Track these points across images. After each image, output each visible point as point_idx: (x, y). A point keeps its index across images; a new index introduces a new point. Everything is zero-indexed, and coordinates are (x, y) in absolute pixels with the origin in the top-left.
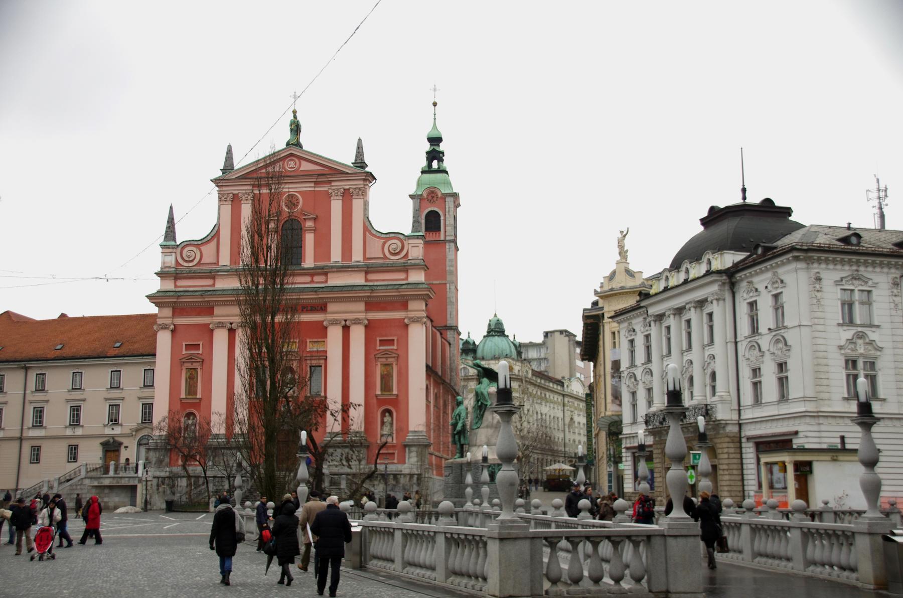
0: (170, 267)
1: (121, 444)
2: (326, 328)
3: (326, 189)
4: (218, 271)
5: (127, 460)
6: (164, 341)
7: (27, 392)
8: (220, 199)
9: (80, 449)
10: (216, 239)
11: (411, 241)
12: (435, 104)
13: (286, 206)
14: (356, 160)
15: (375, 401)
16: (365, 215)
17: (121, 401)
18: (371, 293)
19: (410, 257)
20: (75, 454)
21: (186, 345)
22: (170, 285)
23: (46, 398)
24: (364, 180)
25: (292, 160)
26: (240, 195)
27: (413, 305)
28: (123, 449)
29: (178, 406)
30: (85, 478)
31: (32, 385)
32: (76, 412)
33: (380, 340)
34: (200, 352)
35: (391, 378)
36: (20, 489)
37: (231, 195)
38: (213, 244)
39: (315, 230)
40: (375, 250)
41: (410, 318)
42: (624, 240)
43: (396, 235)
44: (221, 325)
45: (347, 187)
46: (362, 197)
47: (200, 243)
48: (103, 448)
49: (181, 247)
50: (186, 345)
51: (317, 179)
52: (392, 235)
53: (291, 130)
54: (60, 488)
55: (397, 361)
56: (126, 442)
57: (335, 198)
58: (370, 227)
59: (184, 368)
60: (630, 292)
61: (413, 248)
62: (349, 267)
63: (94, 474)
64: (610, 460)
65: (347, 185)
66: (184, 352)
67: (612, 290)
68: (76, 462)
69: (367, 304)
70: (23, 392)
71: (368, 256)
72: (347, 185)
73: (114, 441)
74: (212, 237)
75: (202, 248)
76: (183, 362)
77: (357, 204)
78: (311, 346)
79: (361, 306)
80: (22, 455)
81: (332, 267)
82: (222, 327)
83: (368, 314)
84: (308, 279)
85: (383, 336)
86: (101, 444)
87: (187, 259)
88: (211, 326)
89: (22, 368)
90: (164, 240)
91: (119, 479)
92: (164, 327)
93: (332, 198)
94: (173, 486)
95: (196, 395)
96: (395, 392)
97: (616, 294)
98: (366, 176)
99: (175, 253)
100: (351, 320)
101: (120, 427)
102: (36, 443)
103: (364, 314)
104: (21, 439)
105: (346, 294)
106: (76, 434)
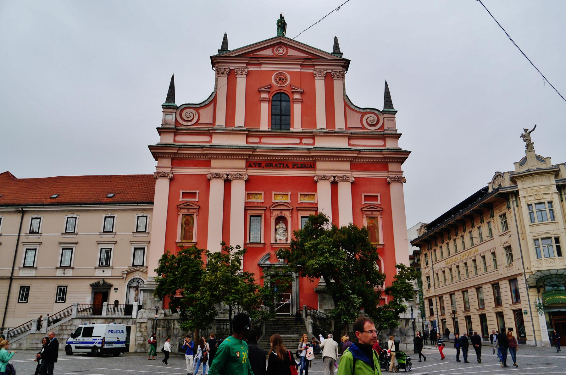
0: (170, 124)
1: (111, 286)
2: (316, 182)
3: (312, 71)
5: (117, 302)
7: (21, 234)
8: (218, 73)
10: (212, 105)
11: (385, 115)
13: (276, 81)
14: (334, 51)
17: (113, 245)
18: (358, 154)
19: (386, 128)
20: (63, 295)
21: (183, 193)
22: (169, 139)
23: (39, 241)
24: (343, 66)
25: (280, 47)
26: (236, 70)
28: (112, 289)
30: (76, 318)
31: (26, 229)
33: (365, 196)
34: (197, 200)
35: (376, 230)
36: (6, 328)
37: (228, 70)
38: (211, 108)
40: (354, 121)
41: (391, 178)
42: (530, 135)
43: (372, 111)
44: (218, 176)
45: (330, 71)
46: (341, 79)
47: (198, 106)
48: (92, 290)
49: (180, 109)
50: (183, 193)
51: (303, 62)
52: (368, 110)
53: (279, 27)
54: (49, 328)
55: (382, 214)
56: (115, 284)
57: (319, 78)
58: (349, 103)
59: (181, 214)
60: (544, 173)
61: (388, 121)
62: (335, 133)
63: (86, 314)
64: (540, 308)
65: (329, 69)
66: (181, 199)
67: (529, 170)
68: (64, 302)
69: (352, 164)
70: (18, 234)
71: (349, 125)
72: (329, 69)
73: (104, 283)
74: (210, 103)
75: (201, 111)
76: (181, 208)
77: (337, 84)
78: (302, 199)
79: (347, 166)
80: (11, 295)
81: (320, 132)
82: (219, 177)
83: (353, 173)
84: (297, 141)
85: (368, 192)
86: (90, 285)
87: (186, 119)
88: (208, 176)
89: (19, 212)
90: (166, 102)
91: (112, 320)
93: (316, 78)
94: (169, 329)
95: (192, 240)
96: (381, 242)
97: (531, 175)
98: (345, 63)
99: (175, 112)
100: (339, 177)
101: (111, 270)
102: (25, 283)
103: (351, 172)
104: (11, 279)
106: (66, 275)
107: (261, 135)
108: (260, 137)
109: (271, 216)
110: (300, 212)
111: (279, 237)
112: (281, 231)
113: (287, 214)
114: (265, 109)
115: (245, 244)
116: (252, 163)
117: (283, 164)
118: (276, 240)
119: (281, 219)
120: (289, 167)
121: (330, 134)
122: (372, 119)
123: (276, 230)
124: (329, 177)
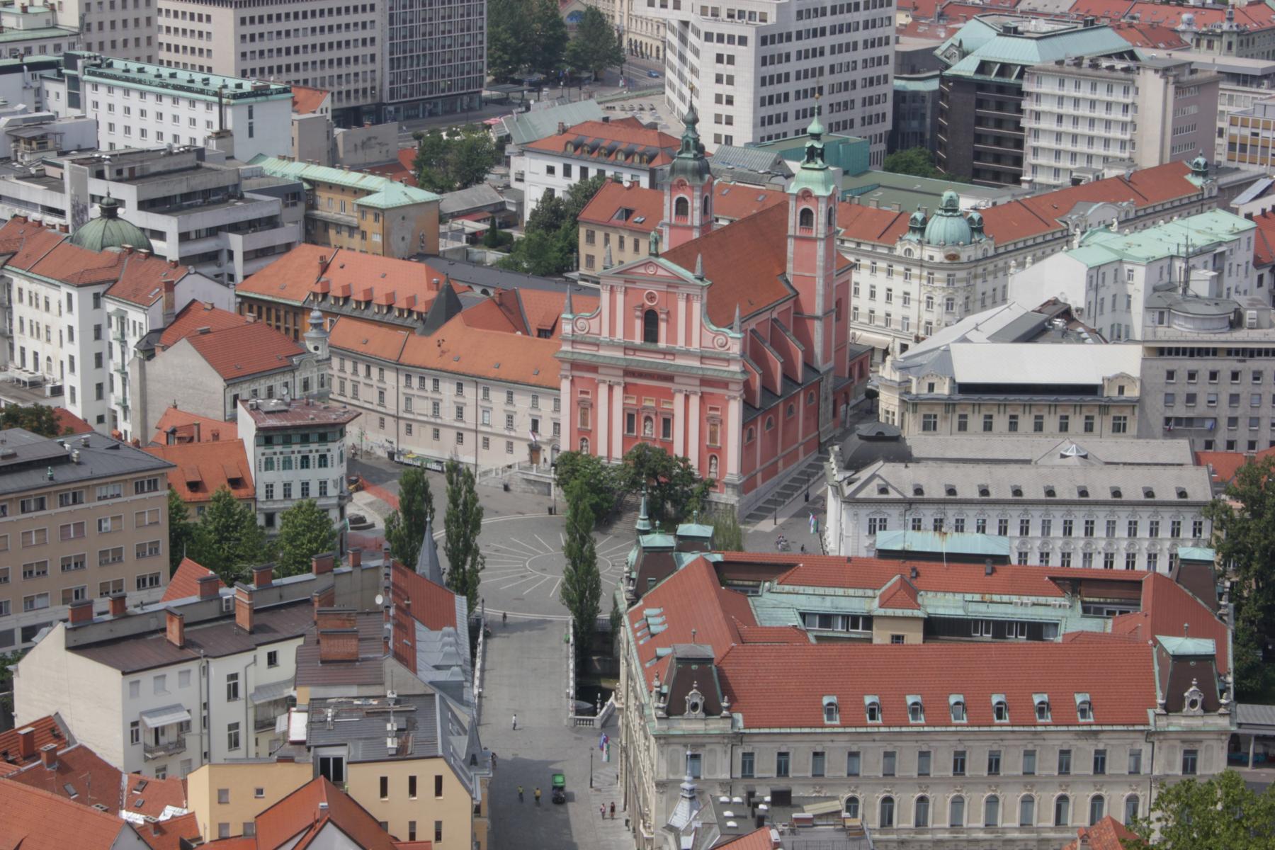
5: (545, 460)
6: (565, 385)
9: (514, 445)
15: (705, 449)
27: (732, 386)
29: (576, 432)
32: (510, 418)
34: (589, 397)
39: (667, 321)
40: (707, 342)
56: (544, 447)
65: (691, 291)
72: (691, 291)
79: (697, 382)
84: (662, 356)
92: (566, 377)
104: (476, 431)
105: (687, 373)
107: (635, 349)
111: (647, 432)
112: (648, 428)
113: (653, 417)
115: (623, 435)
119: (648, 418)
121: (687, 354)
122: (720, 341)
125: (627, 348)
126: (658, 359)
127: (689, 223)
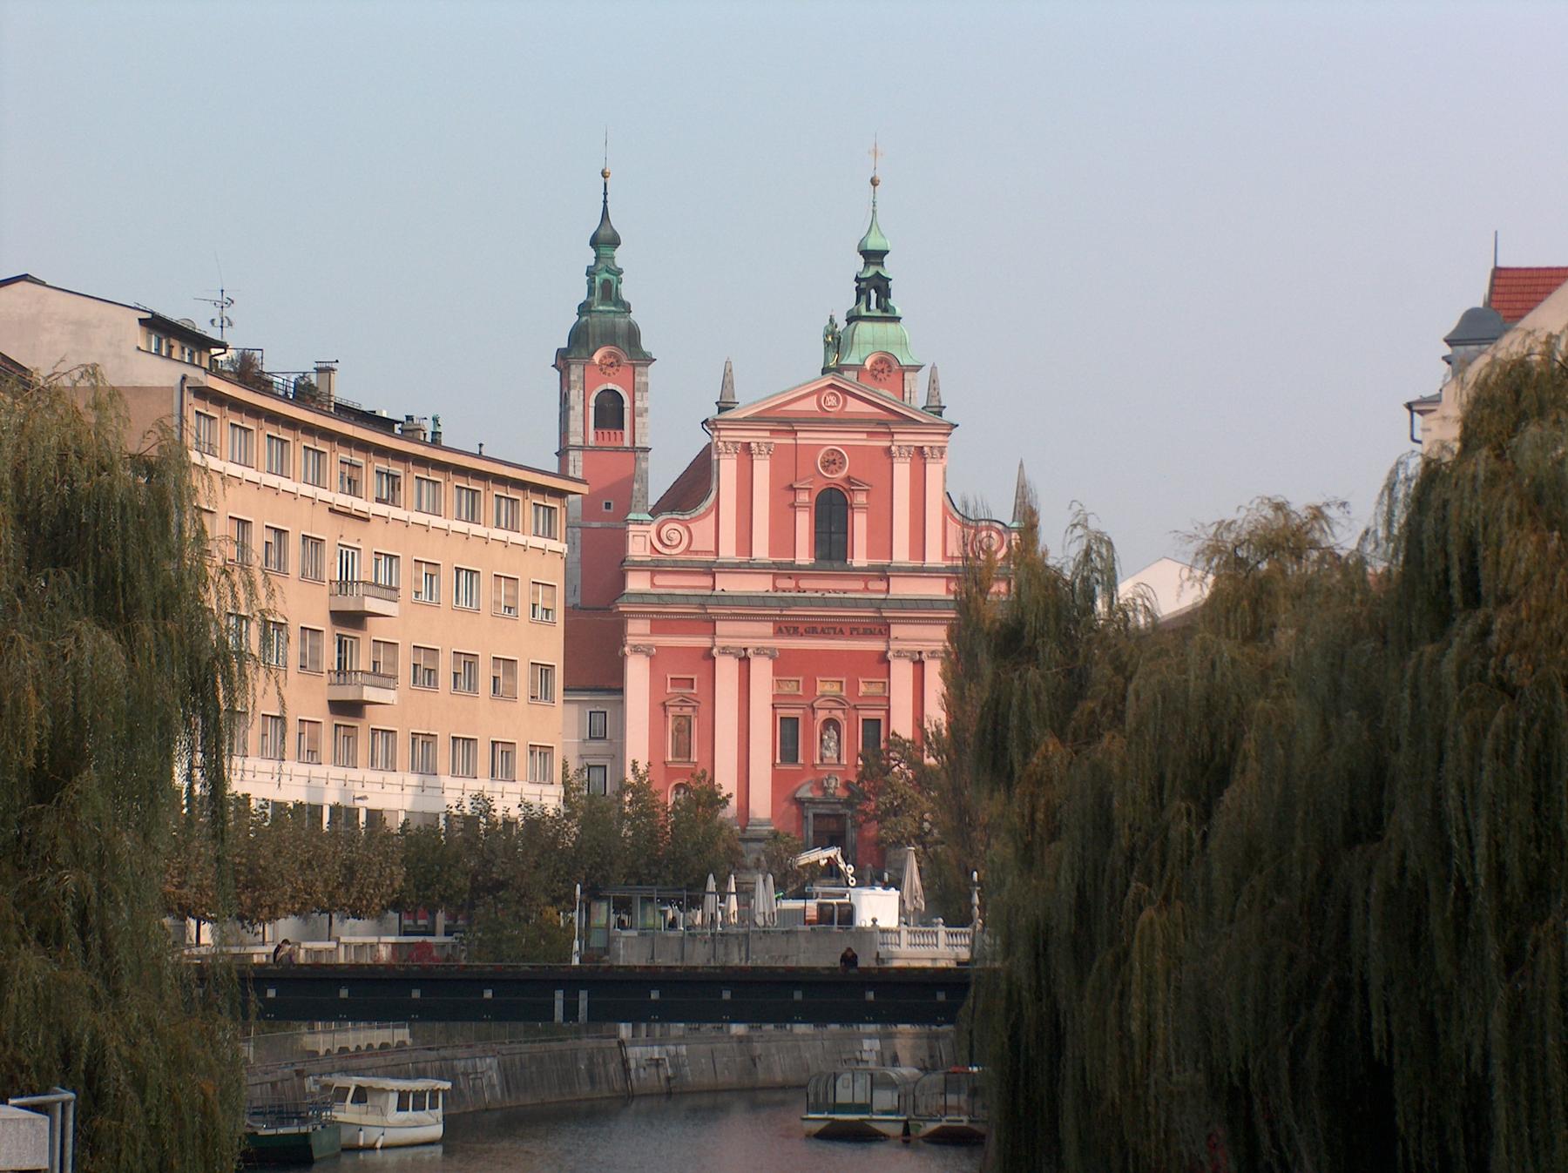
3: (889, 444)
4: (722, 565)
12: (874, 182)
16: (944, 489)
53: (827, 344)
66: (669, 690)
77: (933, 470)
81: (899, 569)
84: (860, 585)
87: (668, 543)
92: (636, 649)
108: (798, 577)
109: (814, 719)
110: (861, 712)
111: (828, 754)
113: (838, 714)
114: (804, 523)
115: (774, 765)
116: (785, 628)
117: (835, 629)
118: (822, 759)
120: (843, 633)
123: (822, 740)
124: (913, 652)
125: (779, 570)
126: (853, 588)
127: (627, 443)
